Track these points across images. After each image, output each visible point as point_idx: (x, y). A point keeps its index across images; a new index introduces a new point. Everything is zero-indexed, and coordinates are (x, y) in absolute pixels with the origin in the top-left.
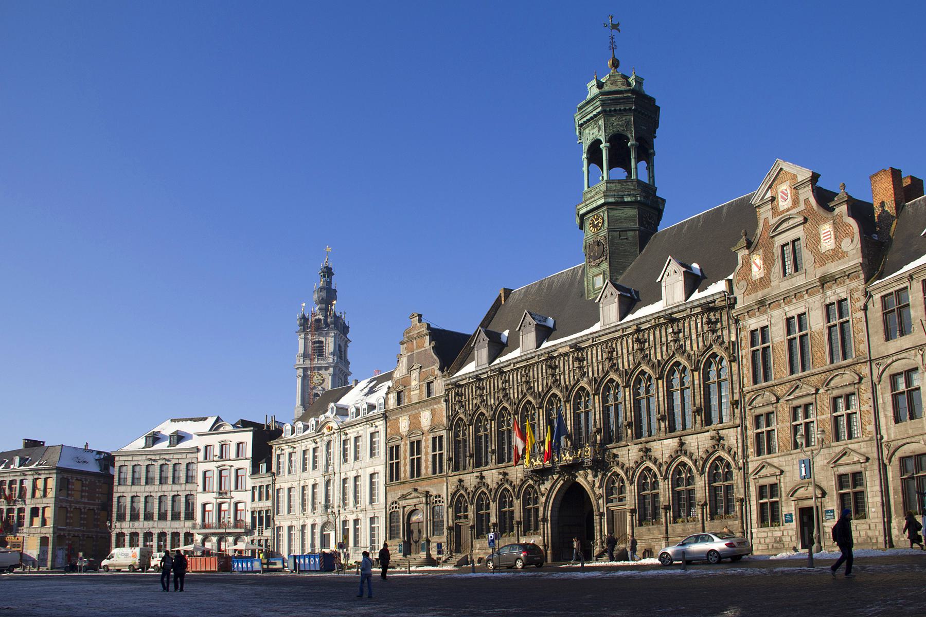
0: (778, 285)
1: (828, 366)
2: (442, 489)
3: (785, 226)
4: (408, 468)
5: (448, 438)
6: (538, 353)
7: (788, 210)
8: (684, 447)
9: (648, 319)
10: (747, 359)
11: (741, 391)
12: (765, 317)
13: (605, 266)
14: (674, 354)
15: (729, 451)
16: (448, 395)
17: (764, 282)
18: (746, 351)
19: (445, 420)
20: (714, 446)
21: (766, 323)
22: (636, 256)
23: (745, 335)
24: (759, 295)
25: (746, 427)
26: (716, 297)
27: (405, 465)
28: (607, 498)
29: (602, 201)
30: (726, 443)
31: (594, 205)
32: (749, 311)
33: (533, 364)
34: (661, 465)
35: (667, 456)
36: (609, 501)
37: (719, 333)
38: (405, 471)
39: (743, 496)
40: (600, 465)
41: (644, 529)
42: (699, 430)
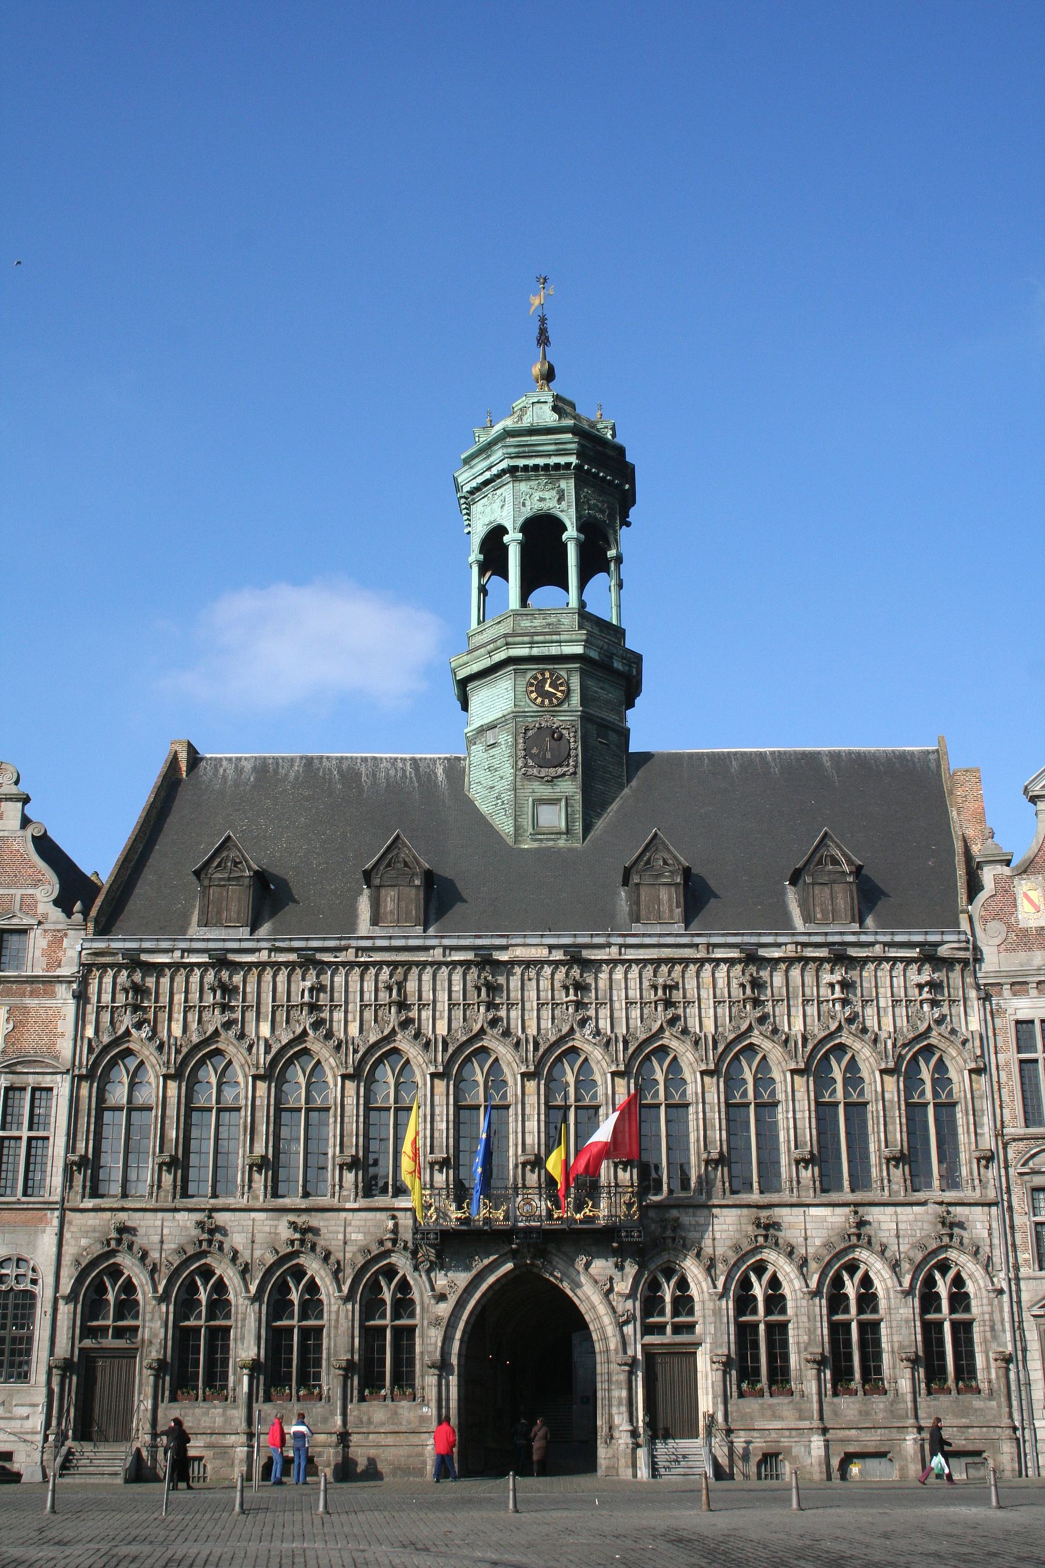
2: (32, 1245)
5: (74, 1101)
6: (446, 942)
8: (866, 1230)
9: (781, 939)
10: (1009, 1074)
11: (999, 1134)
13: (570, 788)
14: (840, 1028)
15: (976, 1253)
16: (84, 983)
18: (1009, 1057)
19: (65, 1048)
20: (940, 1237)
22: (622, 787)
23: (1006, 1026)
25: (1010, 1208)
26: (946, 938)
28: (643, 1324)
29: (578, 649)
30: (965, 1234)
31: (554, 650)
32: (1019, 987)
33: (423, 965)
34: (804, 1263)
35: (818, 1242)
36: (648, 1329)
37: (945, 1010)
39: (1010, 1348)
40: (653, 1241)
41: (752, 1405)
42: (901, 1198)
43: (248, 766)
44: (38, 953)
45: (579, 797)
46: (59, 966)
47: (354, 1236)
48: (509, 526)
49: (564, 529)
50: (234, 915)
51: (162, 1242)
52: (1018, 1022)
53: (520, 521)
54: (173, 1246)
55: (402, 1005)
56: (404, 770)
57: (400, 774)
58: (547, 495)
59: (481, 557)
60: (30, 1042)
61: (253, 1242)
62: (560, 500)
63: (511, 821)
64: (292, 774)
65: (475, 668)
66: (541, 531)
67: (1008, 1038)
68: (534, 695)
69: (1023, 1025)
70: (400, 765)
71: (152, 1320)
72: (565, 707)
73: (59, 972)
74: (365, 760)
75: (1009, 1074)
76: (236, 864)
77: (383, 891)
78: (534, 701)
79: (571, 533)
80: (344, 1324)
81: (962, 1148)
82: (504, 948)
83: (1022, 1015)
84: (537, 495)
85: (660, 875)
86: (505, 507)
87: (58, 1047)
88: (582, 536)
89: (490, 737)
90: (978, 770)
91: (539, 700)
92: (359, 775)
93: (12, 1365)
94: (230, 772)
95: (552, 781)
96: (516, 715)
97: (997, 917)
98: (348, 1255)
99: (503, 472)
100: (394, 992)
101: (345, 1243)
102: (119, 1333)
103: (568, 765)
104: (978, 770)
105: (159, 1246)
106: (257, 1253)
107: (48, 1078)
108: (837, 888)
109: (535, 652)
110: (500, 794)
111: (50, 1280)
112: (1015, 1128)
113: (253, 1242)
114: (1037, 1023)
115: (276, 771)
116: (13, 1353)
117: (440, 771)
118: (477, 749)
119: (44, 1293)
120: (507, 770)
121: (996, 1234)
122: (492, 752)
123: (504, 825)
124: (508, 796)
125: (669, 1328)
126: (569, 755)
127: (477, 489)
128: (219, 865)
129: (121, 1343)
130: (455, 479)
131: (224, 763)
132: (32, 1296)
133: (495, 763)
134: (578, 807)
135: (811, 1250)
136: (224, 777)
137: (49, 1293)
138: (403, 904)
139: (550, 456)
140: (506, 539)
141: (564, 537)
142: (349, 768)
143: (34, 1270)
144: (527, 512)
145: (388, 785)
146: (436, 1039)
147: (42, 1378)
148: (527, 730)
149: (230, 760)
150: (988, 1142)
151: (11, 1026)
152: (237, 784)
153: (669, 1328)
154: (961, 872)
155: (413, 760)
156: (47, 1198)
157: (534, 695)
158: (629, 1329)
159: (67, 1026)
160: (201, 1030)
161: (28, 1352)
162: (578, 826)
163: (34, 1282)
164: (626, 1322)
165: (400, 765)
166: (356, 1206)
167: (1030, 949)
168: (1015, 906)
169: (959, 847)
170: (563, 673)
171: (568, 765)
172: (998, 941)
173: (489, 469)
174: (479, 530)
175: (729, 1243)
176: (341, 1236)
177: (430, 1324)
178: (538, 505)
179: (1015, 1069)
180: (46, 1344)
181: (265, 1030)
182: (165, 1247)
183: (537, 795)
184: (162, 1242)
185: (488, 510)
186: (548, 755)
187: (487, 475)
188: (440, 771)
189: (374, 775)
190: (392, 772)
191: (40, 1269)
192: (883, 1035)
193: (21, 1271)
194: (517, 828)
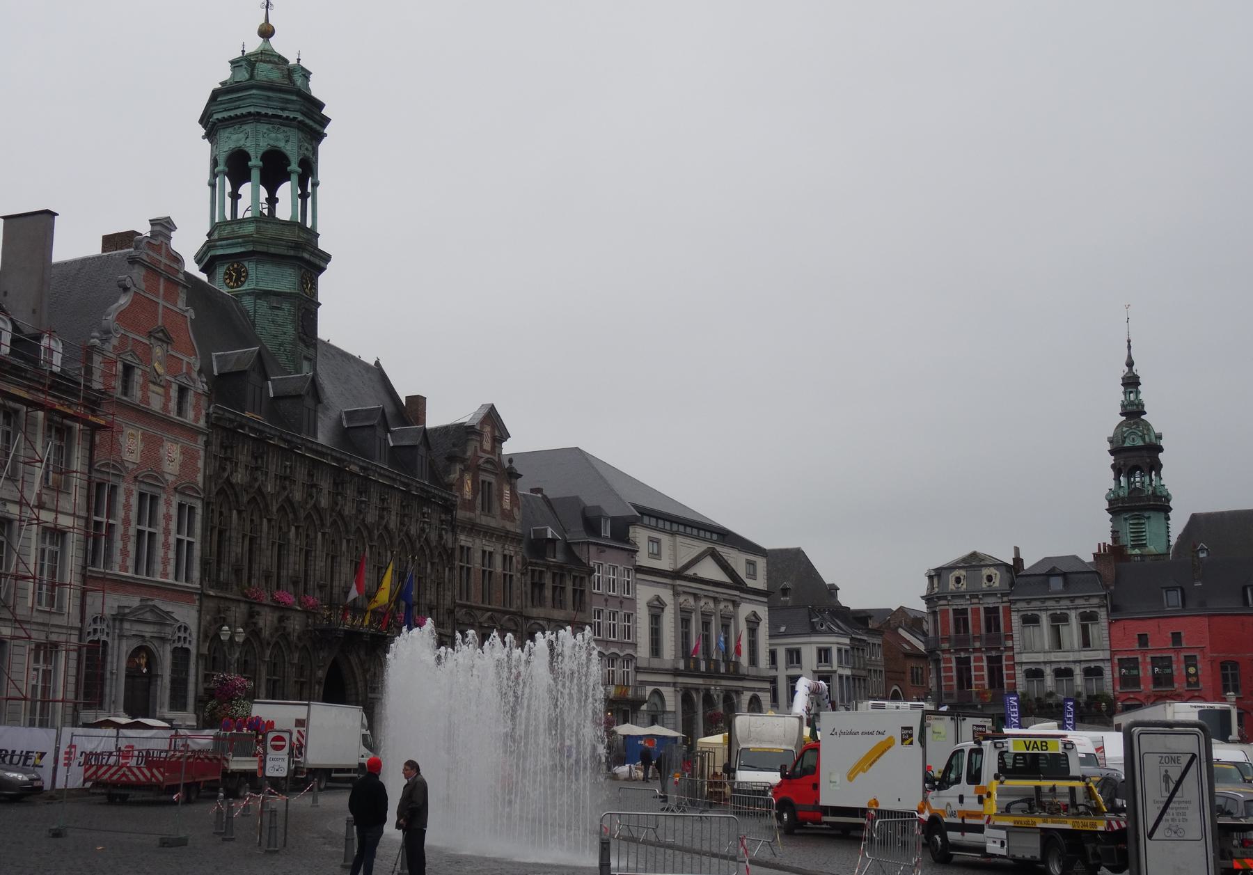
32: (463, 529)
59: (261, 164)
65: (272, 250)
69: (462, 547)
83: (463, 543)
99: (295, 119)
120: (290, 329)
122: (276, 312)
159: (200, 464)
173: (283, 109)
187: (280, 113)
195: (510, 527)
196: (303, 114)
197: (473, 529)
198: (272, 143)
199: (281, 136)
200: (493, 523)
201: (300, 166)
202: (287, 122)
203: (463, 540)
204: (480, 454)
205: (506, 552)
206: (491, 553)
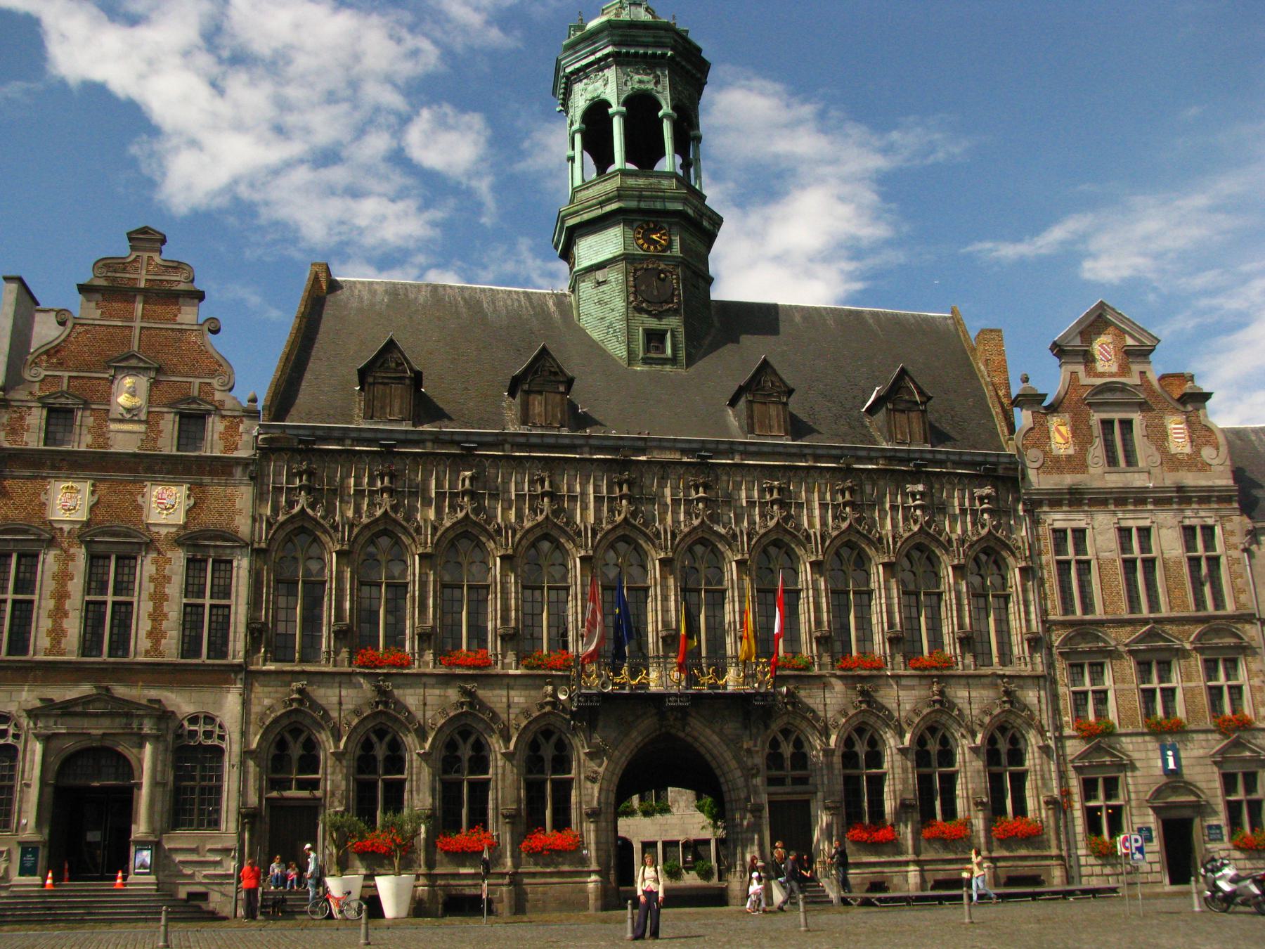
0: (1098, 476)
1: (1192, 611)
2: (219, 704)
3: (1108, 396)
4: (73, 626)
7: (1112, 375)
12: (1082, 516)
17: (1077, 463)
18: (1049, 558)
21: (1082, 525)
24: (1068, 480)
27: (59, 613)
29: (679, 207)
31: (659, 205)
32: (1056, 500)
35: (908, 707)
38: (57, 633)
43: (380, 289)
44: (216, 436)
45: (682, 330)
46: (236, 449)
47: (516, 700)
48: (613, 100)
49: (660, 108)
50: (396, 409)
51: (340, 703)
52: (1055, 531)
53: (623, 97)
54: (351, 707)
55: (553, 496)
56: (519, 301)
57: (516, 304)
58: (645, 78)
60: (209, 519)
61: (425, 704)
62: (657, 83)
63: (624, 347)
64: (421, 300)
65: (586, 217)
66: (640, 108)
67: (1048, 543)
68: (641, 241)
69: (1059, 535)
70: (515, 297)
71: (333, 773)
72: (668, 253)
73: (236, 454)
74: (484, 290)
75: (1049, 572)
76: (398, 364)
77: (531, 397)
78: (641, 246)
79: (666, 109)
80: (510, 778)
81: (1013, 632)
82: (643, 451)
83: (1058, 525)
84: (637, 77)
85: (770, 395)
86: (609, 86)
87: (236, 522)
88: (675, 115)
89: (600, 275)
90: (1000, 331)
91: (646, 246)
92: (479, 302)
93: (202, 812)
94: (366, 295)
95: (659, 316)
96: (626, 258)
97: (1035, 445)
98: (512, 716)
99: (608, 56)
100: (547, 483)
101: (509, 706)
102: (302, 785)
103: (672, 302)
104: (1000, 331)
105: (337, 707)
106: (429, 714)
107: (228, 551)
108: (913, 415)
109: (643, 205)
110: (611, 323)
111: (236, 736)
112: (1056, 615)
113: (425, 704)
114: (1069, 532)
115: (406, 295)
116: (202, 802)
117: (551, 303)
118: (586, 287)
119: (232, 748)
120: (619, 303)
121: (1043, 700)
122: (602, 288)
123: (618, 349)
124: (620, 326)
125: (789, 780)
126: (673, 295)
127: (579, 70)
128: (382, 365)
129: (305, 794)
130: (558, 62)
131: (359, 286)
132: (219, 752)
133: (606, 298)
134: (681, 337)
135: (903, 714)
136: (361, 298)
137: (236, 748)
138: (549, 408)
139: (646, 45)
140: (610, 111)
141: (660, 114)
142: (471, 297)
143: (221, 726)
144: (628, 90)
145: (508, 312)
146: (586, 528)
147: (233, 826)
148: (636, 270)
149: (363, 283)
150: (1035, 626)
151: (192, 502)
152: (372, 305)
153: (789, 780)
154: (996, 410)
155: (525, 293)
156: (230, 660)
157: (641, 241)
158: (758, 781)
160: (371, 514)
161: (218, 802)
162: (682, 354)
163: (222, 738)
164: (754, 776)
165: (515, 297)
166: (518, 672)
167: (1062, 472)
168: (1049, 438)
169: (989, 393)
170: (665, 225)
171: (672, 302)
172: (1037, 465)
173: (593, 53)
174: (580, 100)
175: (837, 707)
176: (504, 700)
177: (587, 778)
178: (637, 86)
179: (1054, 568)
180: (234, 793)
181: (432, 514)
182: (344, 707)
183: (647, 326)
184: (340, 703)
185: (591, 88)
186: (655, 293)
187: (592, 58)
188: (551, 303)
189: (494, 303)
190: (509, 302)
191: (227, 725)
192: (954, 537)
193: (209, 728)
194: (630, 352)
195: (1191, 479)
196: (614, 45)
197: (1075, 498)
198: (589, 96)
199: (600, 84)
200: (1139, 481)
201: (625, 103)
202: (600, 65)
203: (1057, 519)
204: (1084, 380)
205: (1187, 522)
206: (1145, 532)
